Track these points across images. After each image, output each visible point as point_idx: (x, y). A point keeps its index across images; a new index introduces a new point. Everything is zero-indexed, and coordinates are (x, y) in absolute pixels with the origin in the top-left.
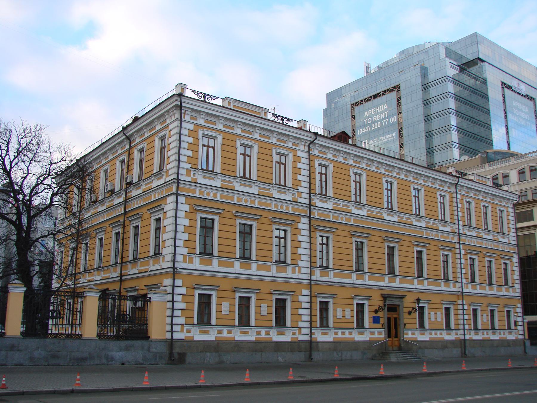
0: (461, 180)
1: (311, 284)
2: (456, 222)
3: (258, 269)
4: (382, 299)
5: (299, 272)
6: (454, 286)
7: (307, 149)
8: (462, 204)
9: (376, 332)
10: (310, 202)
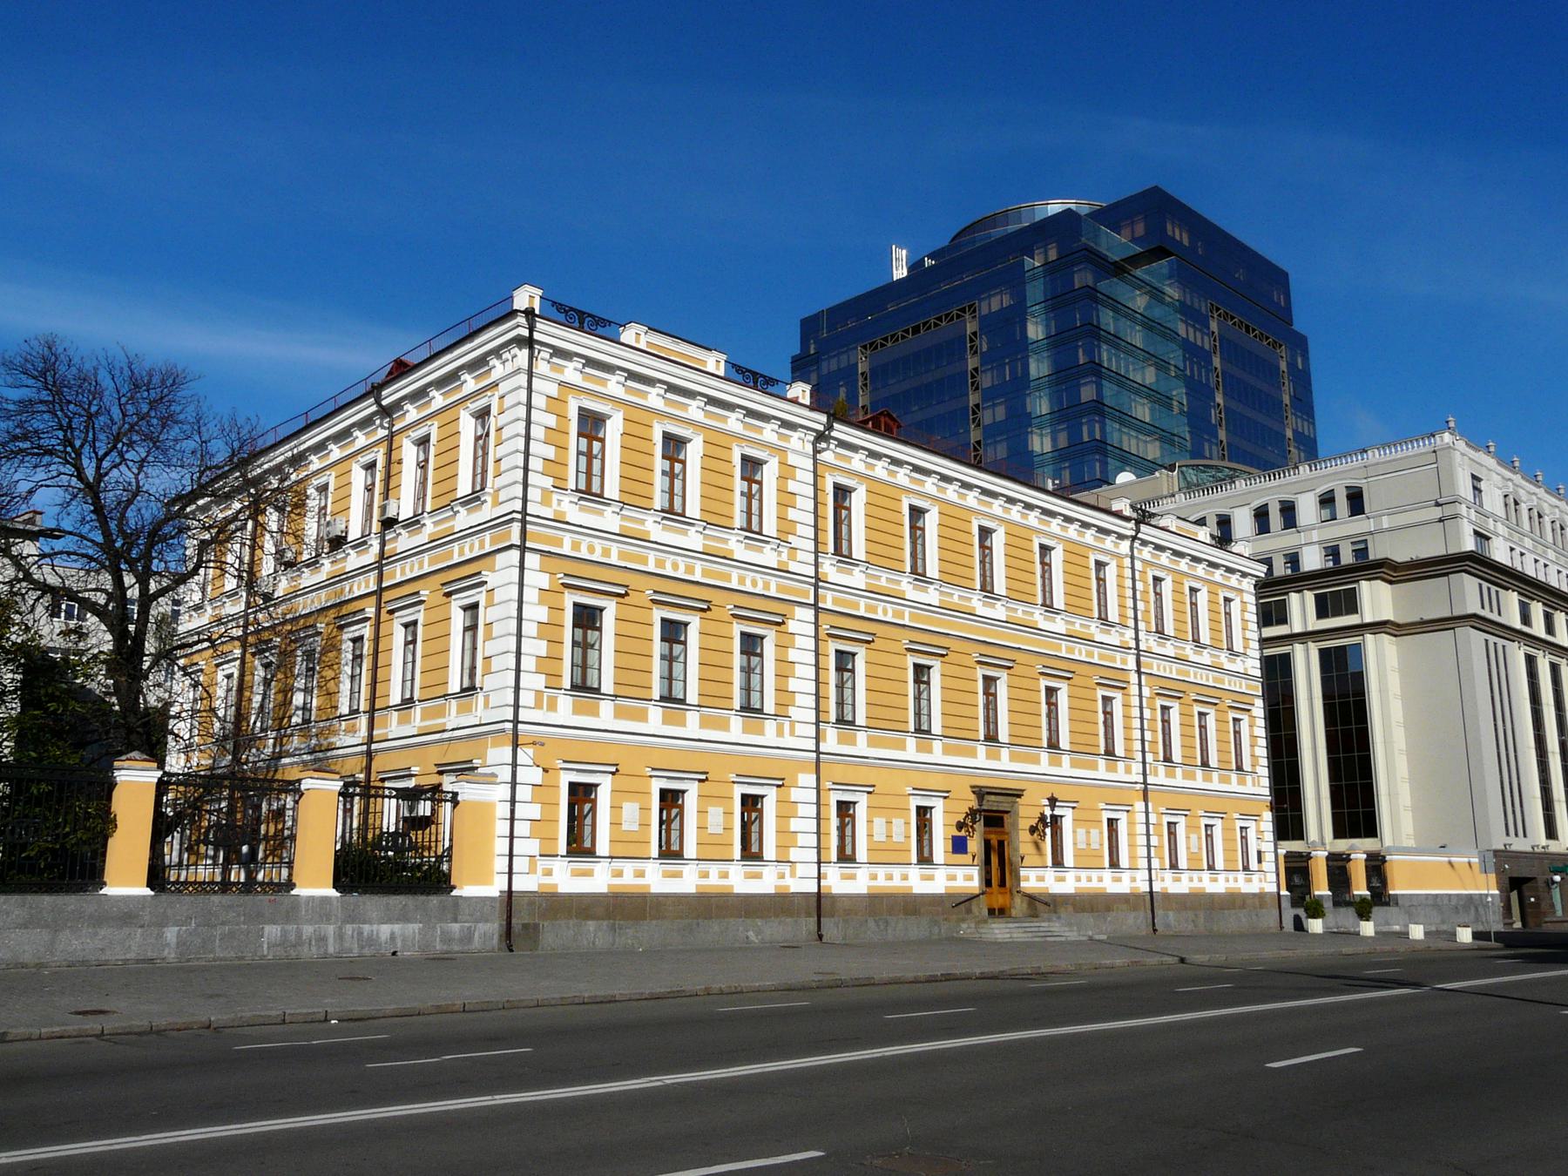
0: (1143, 528)
2: (1131, 623)
4: (973, 797)
5: (792, 733)
6: (1128, 770)
7: (809, 448)
8: (1145, 582)
9: (960, 872)
10: (817, 572)
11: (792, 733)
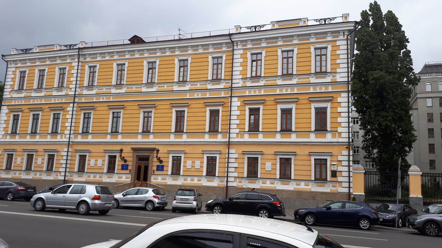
1: (69, 144)
3: (40, 138)
9: (124, 176)
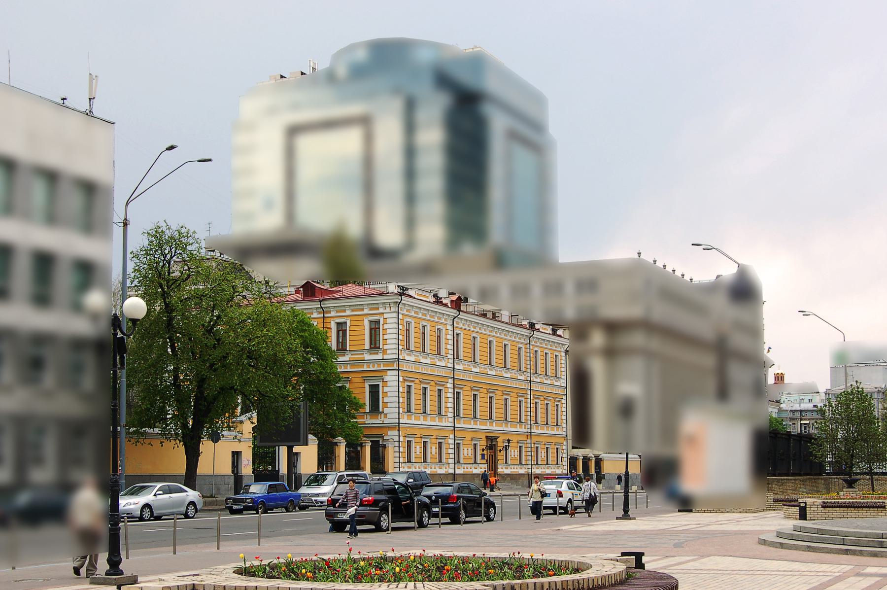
9: (483, 466)
11: (448, 422)
